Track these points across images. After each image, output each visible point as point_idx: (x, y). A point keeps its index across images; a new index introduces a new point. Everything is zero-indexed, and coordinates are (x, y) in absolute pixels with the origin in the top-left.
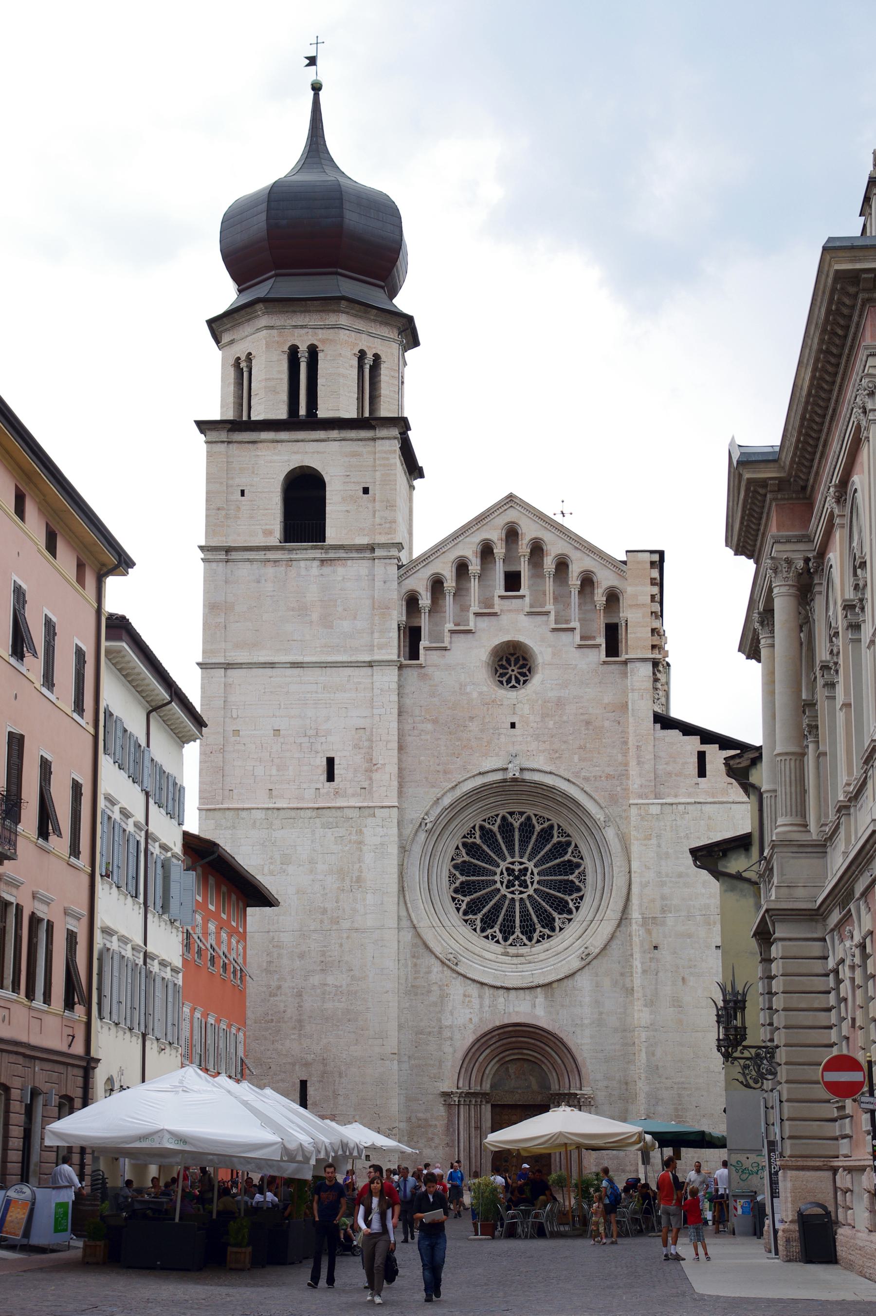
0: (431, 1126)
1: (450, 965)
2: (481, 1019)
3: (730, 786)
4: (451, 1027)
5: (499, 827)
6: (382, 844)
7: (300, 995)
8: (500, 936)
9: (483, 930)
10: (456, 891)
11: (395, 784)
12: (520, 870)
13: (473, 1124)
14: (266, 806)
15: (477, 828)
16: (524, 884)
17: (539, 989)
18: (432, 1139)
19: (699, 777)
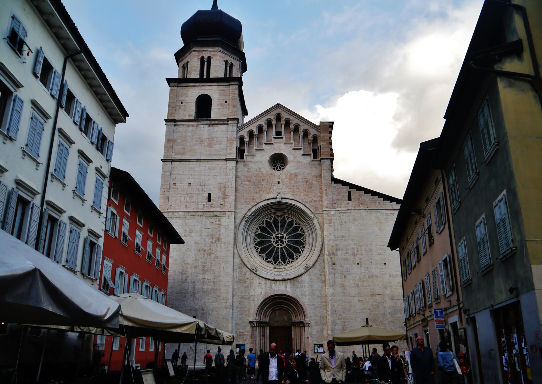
0: (245, 335)
1: (254, 271)
2: (265, 293)
3: (360, 204)
4: (253, 296)
5: (273, 221)
6: (228, 225)
7: (194, 283)
8: (273, 262)
9: (266, 259)
10: (256, 244)
11: (234, 203)
12: (281, 237)
13: (262, 334)
14: (184, 211)
15: (265, 221)
16: (282, 242)
17: (288, 281)
18: (245, 340)
19: (349, 200)
